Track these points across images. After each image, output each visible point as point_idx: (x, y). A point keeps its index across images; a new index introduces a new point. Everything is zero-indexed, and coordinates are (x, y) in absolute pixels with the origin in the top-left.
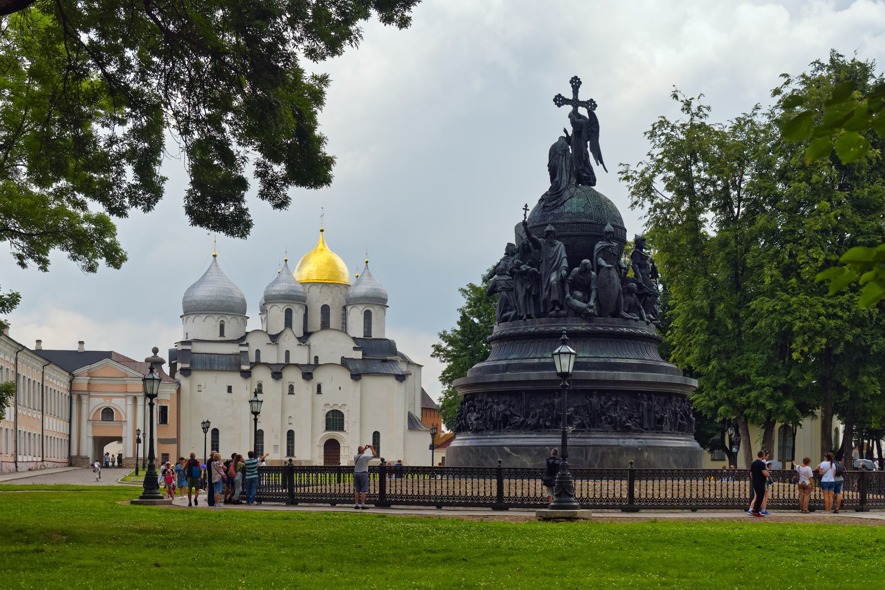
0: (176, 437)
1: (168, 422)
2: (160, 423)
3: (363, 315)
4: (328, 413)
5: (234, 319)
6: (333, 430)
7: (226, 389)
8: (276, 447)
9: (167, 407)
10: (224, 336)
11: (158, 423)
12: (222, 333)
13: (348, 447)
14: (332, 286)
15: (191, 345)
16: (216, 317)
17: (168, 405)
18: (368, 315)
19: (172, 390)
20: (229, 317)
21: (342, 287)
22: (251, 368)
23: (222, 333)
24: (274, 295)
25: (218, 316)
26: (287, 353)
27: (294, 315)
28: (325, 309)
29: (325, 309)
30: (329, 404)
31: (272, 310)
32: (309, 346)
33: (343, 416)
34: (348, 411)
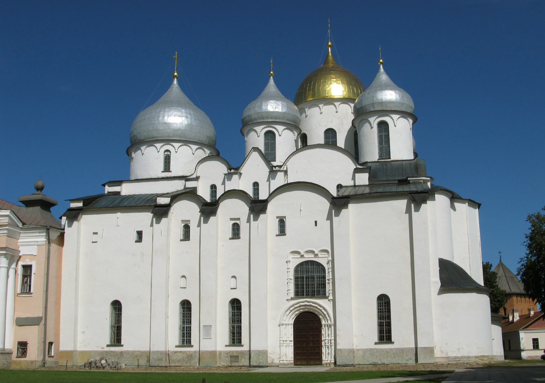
1: (32, 291)
4: (297, 266)
5: (185, 147)
6: (308, 296)
7: (135, 236)
8: (208, 328)
10: (170, 171)
11: (19, 291)
12: (167, 168)
15: (120, 185)
16: (158, 145)
17: (34, 263)
19: (38, 240)
20: (177, 145)
22: (172, 201)
23: (167, 168)
26: (256, 185)
27: (278, 140)
28: (330, 134)
29: (330, 134)
30: (298, 253)
32: (286, 172)
33: (323, 269)
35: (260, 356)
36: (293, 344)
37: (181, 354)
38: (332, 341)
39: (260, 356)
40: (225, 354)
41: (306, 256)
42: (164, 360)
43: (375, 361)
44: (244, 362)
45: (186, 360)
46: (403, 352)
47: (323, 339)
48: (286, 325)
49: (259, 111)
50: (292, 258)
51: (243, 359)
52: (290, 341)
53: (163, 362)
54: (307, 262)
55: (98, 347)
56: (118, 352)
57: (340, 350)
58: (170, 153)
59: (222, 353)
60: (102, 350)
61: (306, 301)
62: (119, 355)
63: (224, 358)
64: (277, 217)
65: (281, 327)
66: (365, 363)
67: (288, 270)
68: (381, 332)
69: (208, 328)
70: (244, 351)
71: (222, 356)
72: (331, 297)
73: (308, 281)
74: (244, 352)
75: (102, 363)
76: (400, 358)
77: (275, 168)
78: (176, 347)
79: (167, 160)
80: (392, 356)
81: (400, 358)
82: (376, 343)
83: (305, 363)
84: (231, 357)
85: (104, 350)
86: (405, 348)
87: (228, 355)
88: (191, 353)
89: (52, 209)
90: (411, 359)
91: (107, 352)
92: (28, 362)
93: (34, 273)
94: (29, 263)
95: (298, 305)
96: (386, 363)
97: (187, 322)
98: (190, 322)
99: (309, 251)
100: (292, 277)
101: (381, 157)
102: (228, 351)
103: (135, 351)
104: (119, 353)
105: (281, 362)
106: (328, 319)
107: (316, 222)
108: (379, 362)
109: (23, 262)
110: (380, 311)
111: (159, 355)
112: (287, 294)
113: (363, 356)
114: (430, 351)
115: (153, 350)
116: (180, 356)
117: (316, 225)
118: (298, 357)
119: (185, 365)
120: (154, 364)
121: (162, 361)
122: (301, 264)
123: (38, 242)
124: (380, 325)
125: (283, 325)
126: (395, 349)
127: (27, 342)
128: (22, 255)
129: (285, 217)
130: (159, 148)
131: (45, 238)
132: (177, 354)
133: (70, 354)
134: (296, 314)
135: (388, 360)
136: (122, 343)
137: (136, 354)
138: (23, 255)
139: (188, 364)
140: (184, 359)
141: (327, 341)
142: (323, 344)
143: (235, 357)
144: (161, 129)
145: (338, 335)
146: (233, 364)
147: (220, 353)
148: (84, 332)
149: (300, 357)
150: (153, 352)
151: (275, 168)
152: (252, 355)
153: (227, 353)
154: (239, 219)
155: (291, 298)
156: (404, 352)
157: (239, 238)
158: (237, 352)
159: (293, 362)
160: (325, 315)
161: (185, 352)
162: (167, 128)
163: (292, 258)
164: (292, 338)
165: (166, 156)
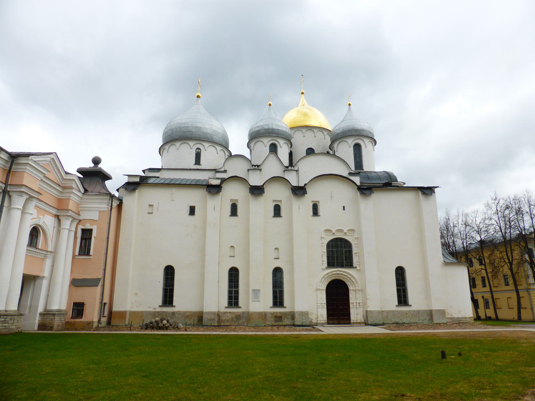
0: (100, 276)
1: (91, 253)
2: (79, 255)
3: (352, 149)
6: (338, 266)
8: (256, 292)
9: (91, 230)
13: (362, 291)
14: (315, 130)
16: (192, 143)
18: (357, 148)
20: (206, 145)
21: (326, 133)
22: (221, 183)
24: (257, 131)
25: (194, 142)
31: (256, 146)
32: (297, 171)
34: (358, 238)
35: (303, 317)
36: (326, 307)
37: (230, 314)
38: (354, 304)
39: (303, 317)
40: (270, 315)
41: (336, 234)
42: (216, 320)
43: (397, 321)
44: (286, 321)
45: (235, 319)
46: (419, 313)
47: (351, 301)
48: (322, 290)
49: (267, 127)
50: (325, 235)
51: (286, 319)
52: (324, 303)
53: (216, 321)
54: (336, 239)
55: (150, 307)
56: (170, 312)
57: (371, 311)
58: (201, 151)
59: (267, 314)
60: (154, 310)
61: (338, 271)
62: (171, 315)
63: (269, 318)
64: (312, 201)
65: (318, 292)
66: (389, 323)
67: (323, 245)
68: (399, 296)
69: (256, 292)
70: (287, 312)
71: (267, 317)
72: (358, 268)
73: (337, 254)
74: (286, 313)
75: (164, 323)
76: (417, 319)
77: (291, 167)
78: (226, 307)
79: (198, 156)
80: (411, 316)
81: (417, 319)
82: (397, 306)
83: (335, 322)
84: (275, 317)
85: (156, 310)
86: (421, 310)
87: (272, 315)
88: (239, 314)
89: (107, 183)
90: (425, 319)
91: (159, 313)
92: (85, 323)
93: (95, 236)
94: (88, 226)
95: (331, 274)
96: (405, 323)
97: (234, 287)
98: (237, 286)
99: (339, 229)
100: (326, 251)
101: (356, 168)
102: (272, 312)
103: (188, 312)
104: (170, 313)
105: (319, 321)
106: (356, 285)
107: (344, 207)
108: (400, 322)
109: (82, 226)
110: (397, 279)
111: (212, 315)
112: (322, 264)
113: (387, 317)
114: (442, 312)
115: (205, 311)
116: (229, 317)
117: (344, 209)
118: (330, 318)
119: (233, 324)
120: (207, 324)
121: (215, 321)
122: (332, 241)
123: (100, 208)
124: (398, 291)
125: (319, 290)
126: (412, 310)
127: (84, 303)
128: (82, 219)
129: (318, 202)
130: (192, 145)
131: (108, 205)
132: (227, 314)
133: (122, 314)
134: (328, 281)
135: (407, 320)
136: (174, 304)
137: (187, 314)
138: (83, 219)
139: (237, 324)
140: (232, 318)
141: (355, 304)
142: (351, 306)
143: (278, 318)
144: (194, 131)
145: (368, 299)
146: (277, 324)
147: (265, 314)
148: (136, 294)
149: (332, 318)
150: (206, 312)
151: (291, 167)
152: (296, 315)
153: (272, 314)
154: (281, 201)
155: (326, 267)
156: (420, 313)
157: (282, 217)
158: (280, 313)
159: (326, 321)
160: (353, 282)
161: (234, 312)
162: (199, 131)
163: (325, 235)
164: (325, 302)
165: (197, 153)
